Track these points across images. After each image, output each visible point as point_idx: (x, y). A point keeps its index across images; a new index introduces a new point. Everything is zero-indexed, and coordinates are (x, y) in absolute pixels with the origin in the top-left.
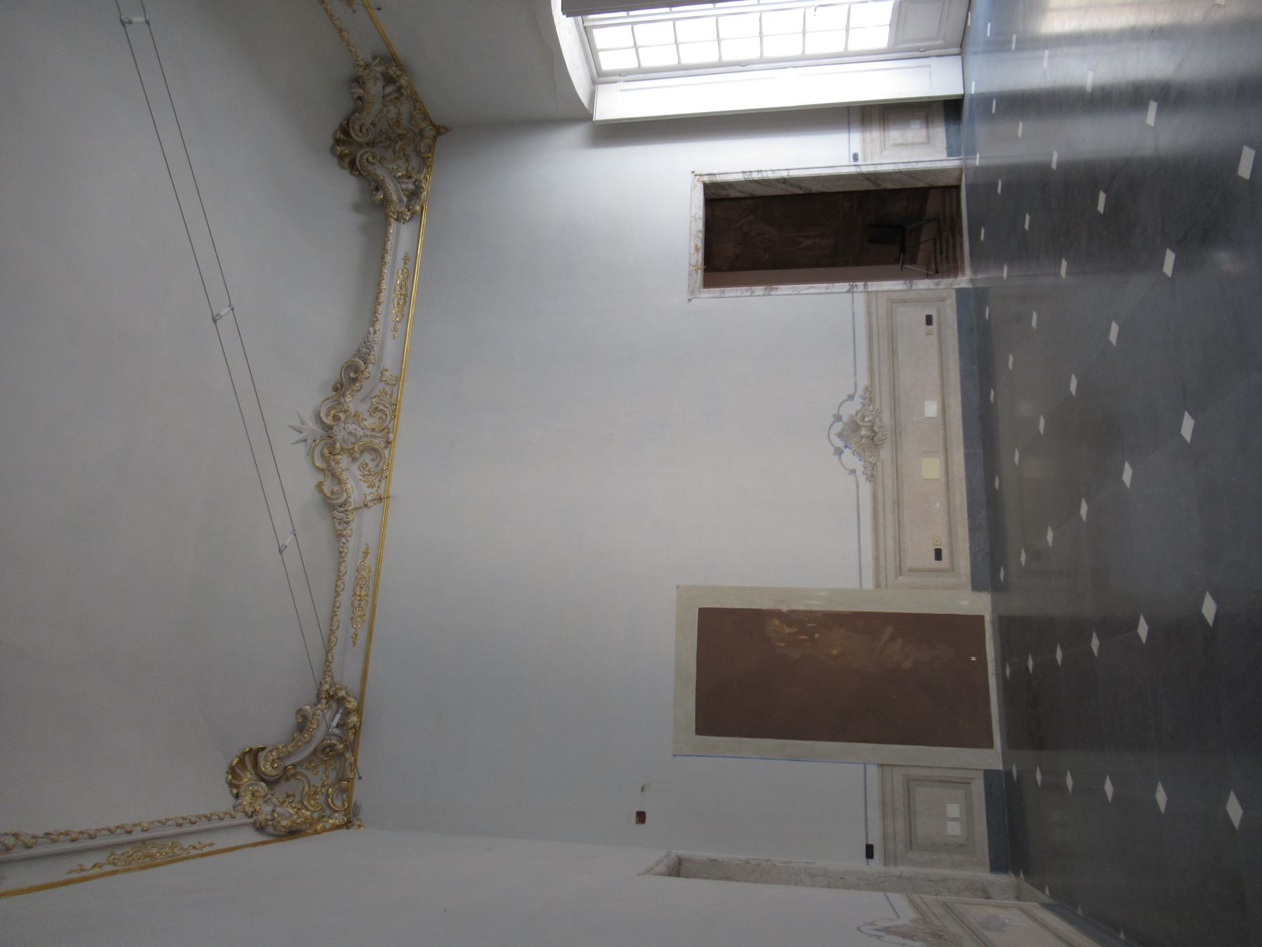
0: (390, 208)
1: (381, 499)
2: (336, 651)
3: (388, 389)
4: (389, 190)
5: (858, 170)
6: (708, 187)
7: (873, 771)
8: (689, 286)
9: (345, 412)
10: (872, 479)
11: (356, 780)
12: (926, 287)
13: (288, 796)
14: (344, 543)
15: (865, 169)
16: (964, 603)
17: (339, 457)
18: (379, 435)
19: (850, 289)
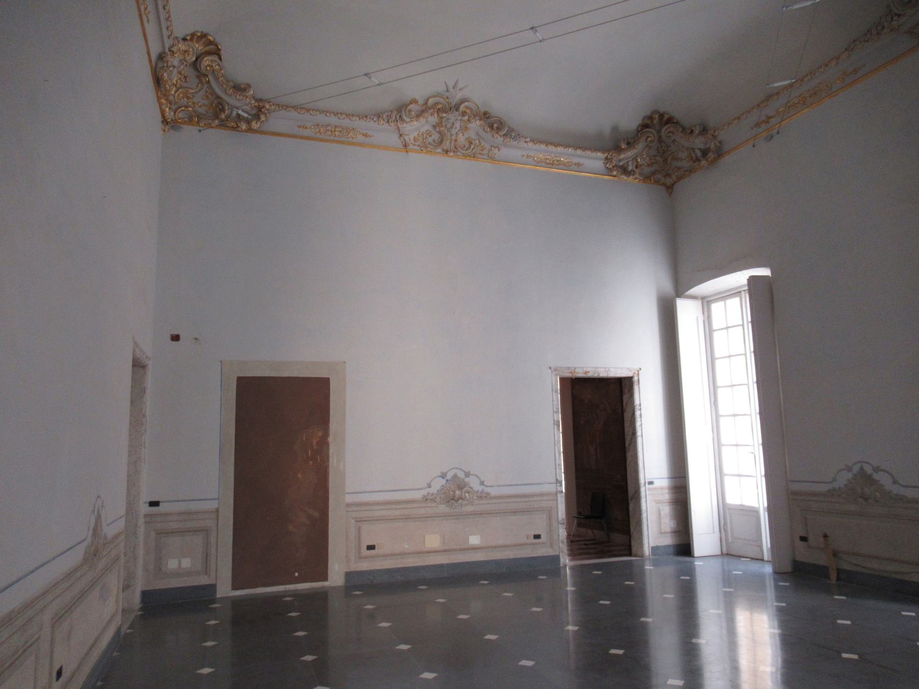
0: (615, 153)
1: (406, 146)
2: (293, 114)
3: (485, 152)
4: (628, 152)
6: (630, 379)
7: (213, 505)
8: (560, 367)
9: (469, 120)
10: (424, 499)
11: (198, 128)
12: (560, 534)
13: (185, 77)
14: (373, 119)
15: (642, 490)
16: (337, 567)
17: (436, 115)
18: (452, 145)
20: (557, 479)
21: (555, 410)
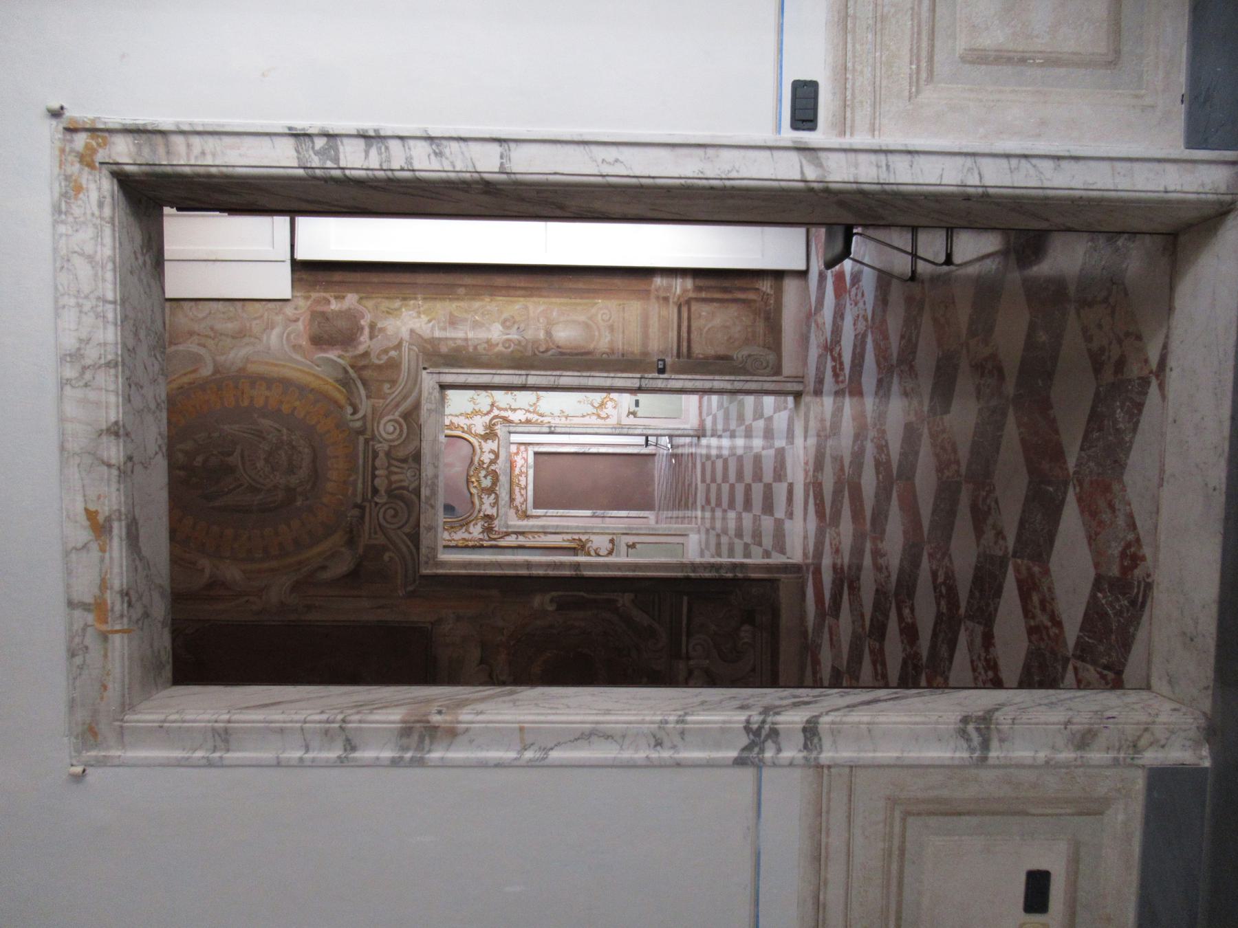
5: (811, 174)
8: (72, 704)
12: (1042, 755)
19: (747, 748)
20: (740, 762)
21: (333, 754)
